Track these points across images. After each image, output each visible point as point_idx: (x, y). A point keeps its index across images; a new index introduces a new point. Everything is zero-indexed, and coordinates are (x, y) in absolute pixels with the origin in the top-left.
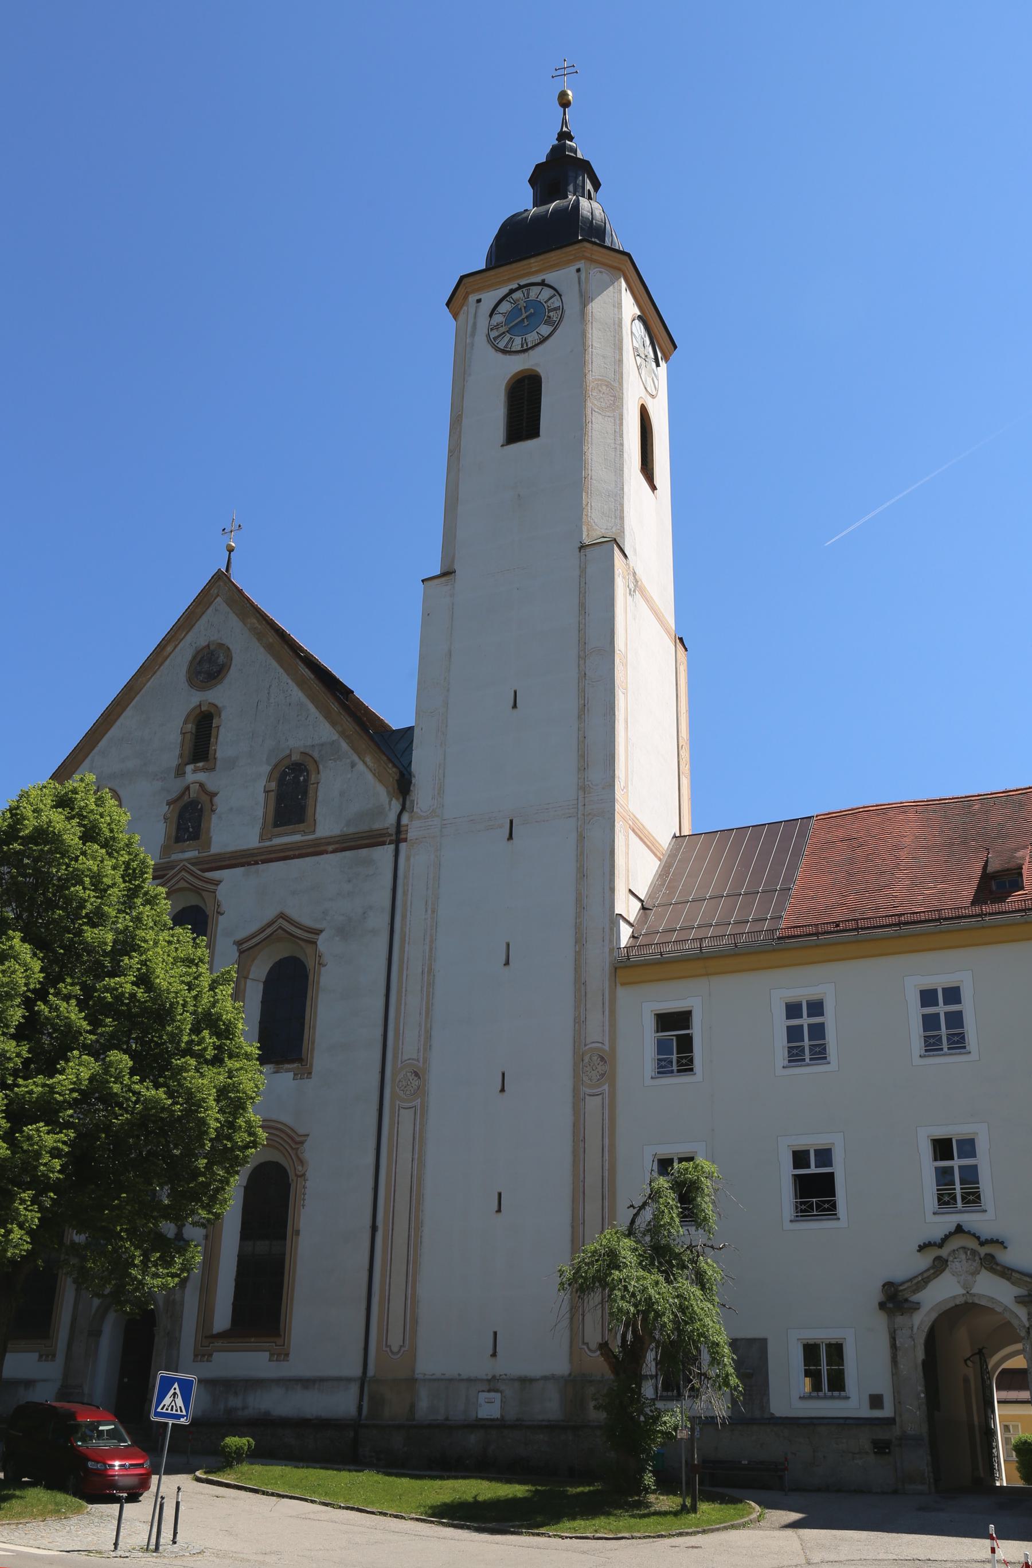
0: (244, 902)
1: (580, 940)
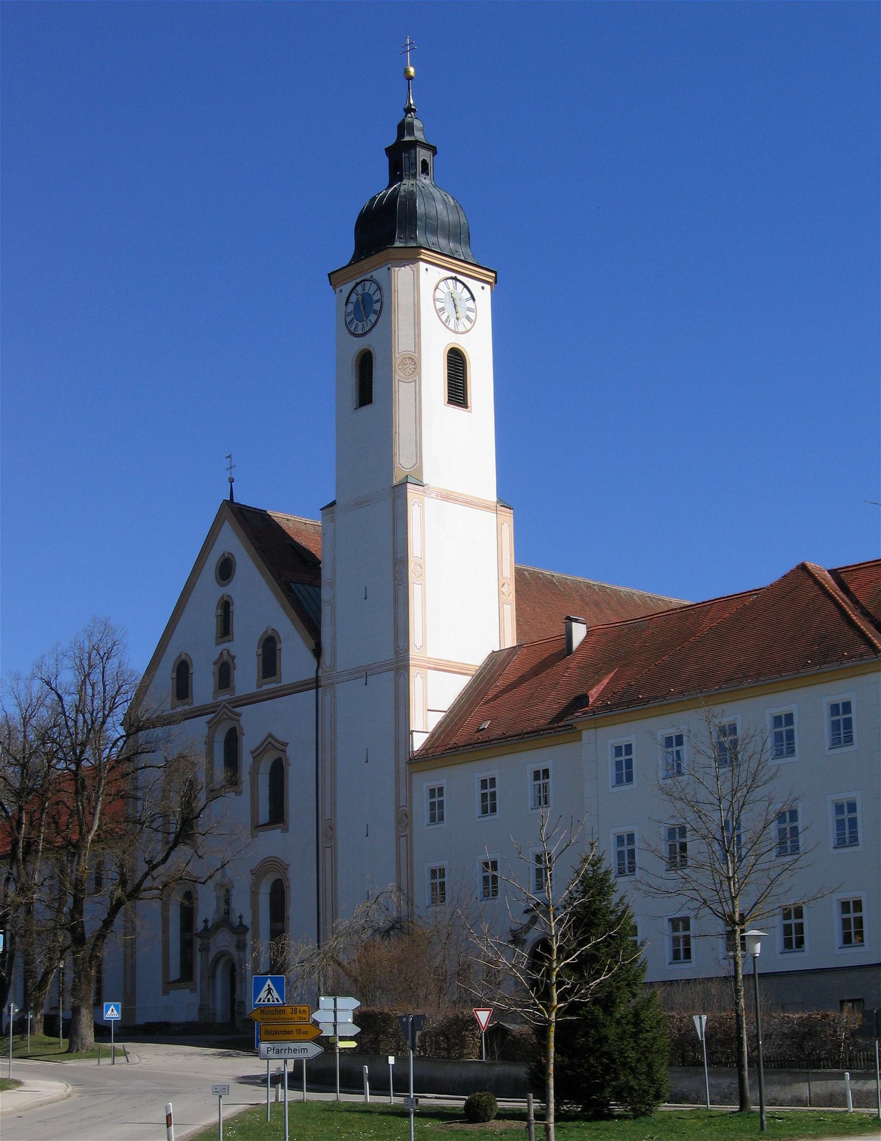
0: (255, 724)
1: (397, 745)
